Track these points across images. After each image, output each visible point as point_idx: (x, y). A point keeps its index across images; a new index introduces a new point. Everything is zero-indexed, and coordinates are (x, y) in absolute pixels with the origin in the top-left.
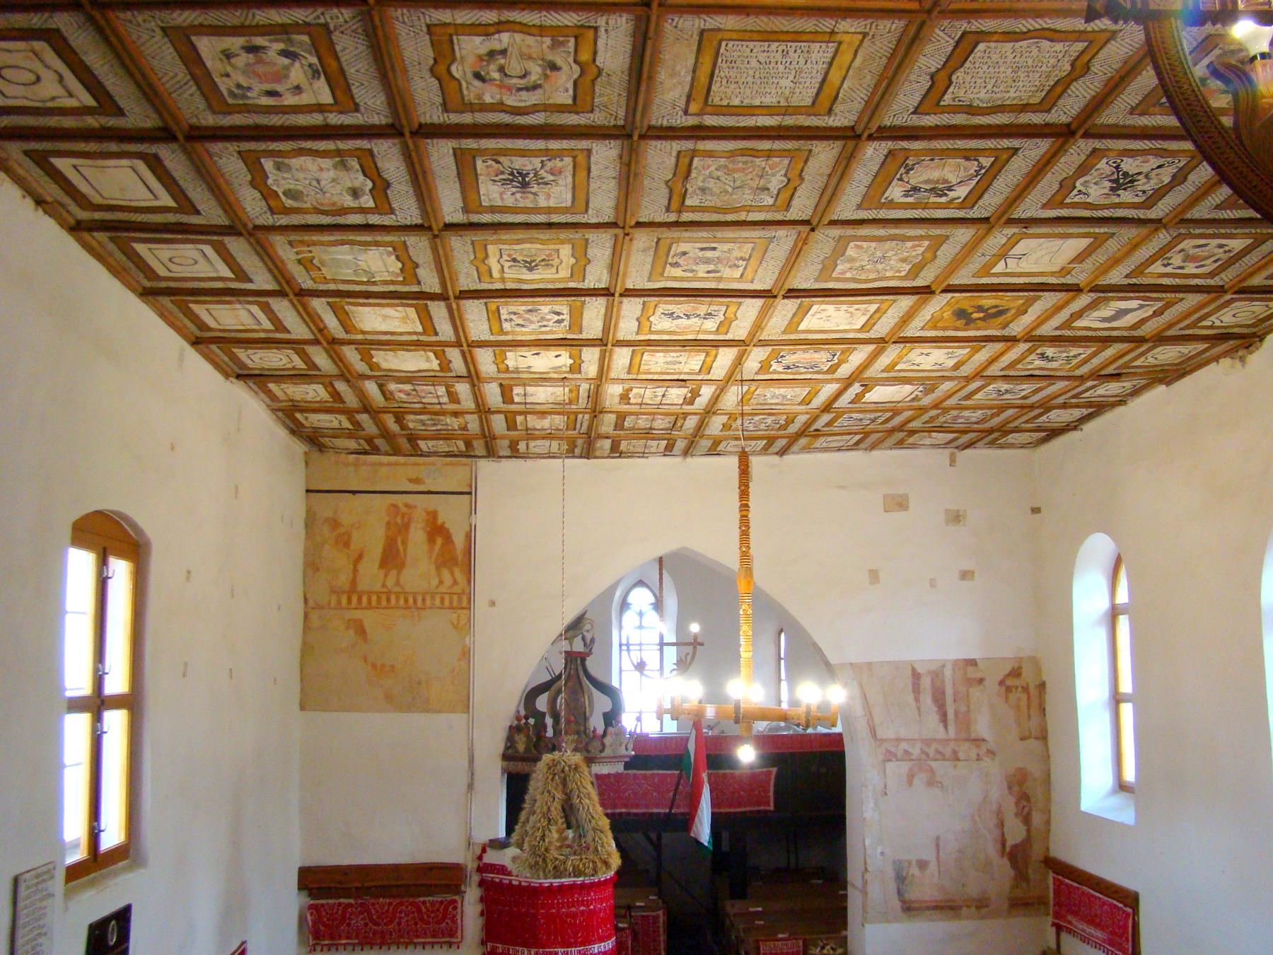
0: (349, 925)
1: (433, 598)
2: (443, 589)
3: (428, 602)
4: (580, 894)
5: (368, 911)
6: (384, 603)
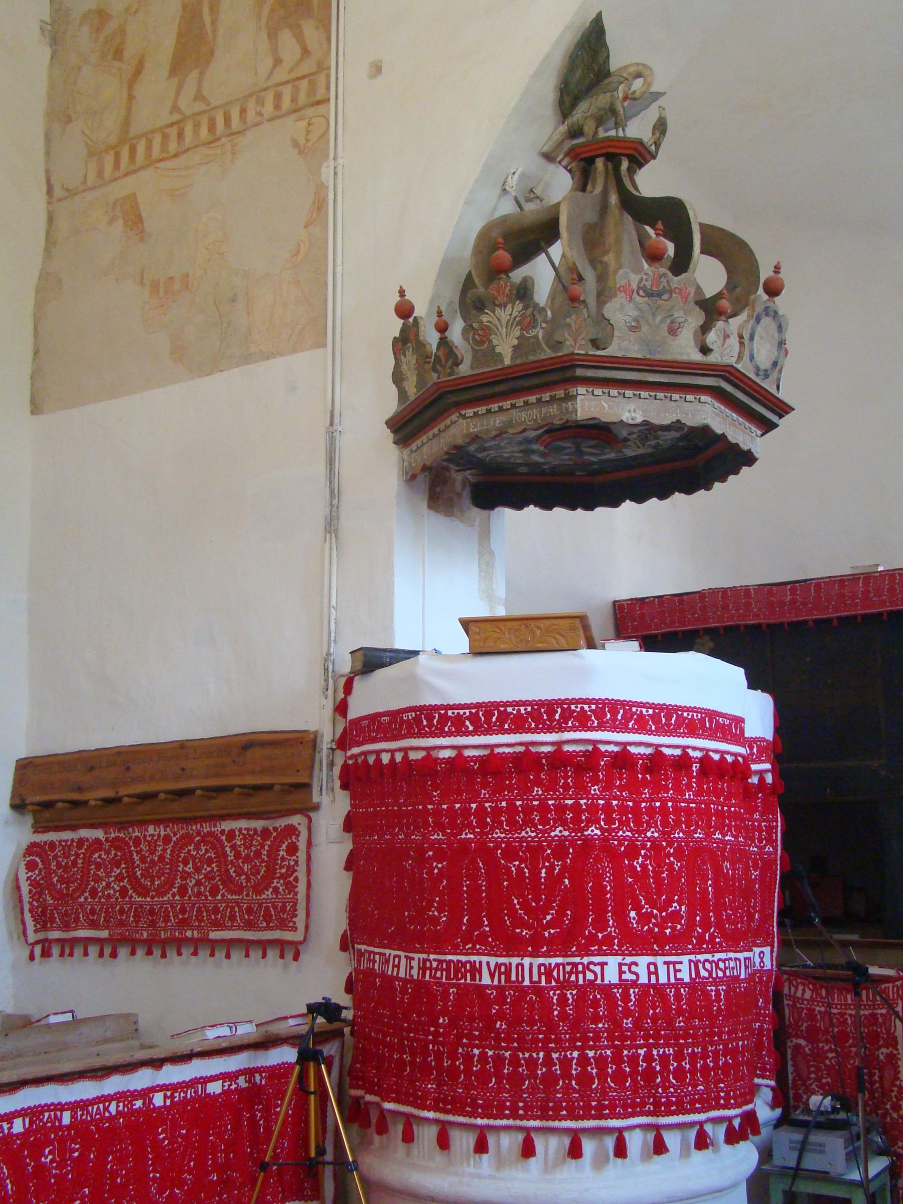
0: (94, 892)
1: (261, 102)
2: (281, 75)
3: (251, 116)
4: (550, 787)
5: (130, 862)
6: (173, 147)
